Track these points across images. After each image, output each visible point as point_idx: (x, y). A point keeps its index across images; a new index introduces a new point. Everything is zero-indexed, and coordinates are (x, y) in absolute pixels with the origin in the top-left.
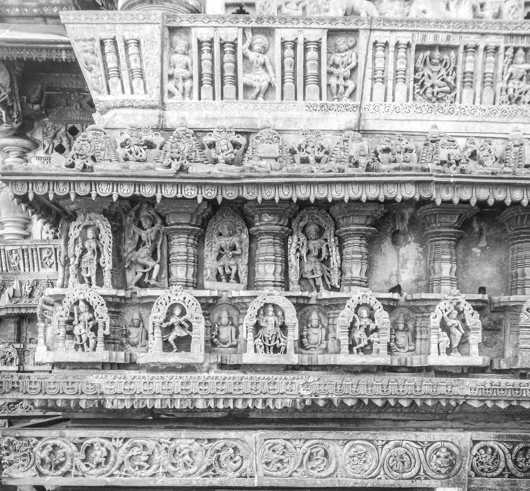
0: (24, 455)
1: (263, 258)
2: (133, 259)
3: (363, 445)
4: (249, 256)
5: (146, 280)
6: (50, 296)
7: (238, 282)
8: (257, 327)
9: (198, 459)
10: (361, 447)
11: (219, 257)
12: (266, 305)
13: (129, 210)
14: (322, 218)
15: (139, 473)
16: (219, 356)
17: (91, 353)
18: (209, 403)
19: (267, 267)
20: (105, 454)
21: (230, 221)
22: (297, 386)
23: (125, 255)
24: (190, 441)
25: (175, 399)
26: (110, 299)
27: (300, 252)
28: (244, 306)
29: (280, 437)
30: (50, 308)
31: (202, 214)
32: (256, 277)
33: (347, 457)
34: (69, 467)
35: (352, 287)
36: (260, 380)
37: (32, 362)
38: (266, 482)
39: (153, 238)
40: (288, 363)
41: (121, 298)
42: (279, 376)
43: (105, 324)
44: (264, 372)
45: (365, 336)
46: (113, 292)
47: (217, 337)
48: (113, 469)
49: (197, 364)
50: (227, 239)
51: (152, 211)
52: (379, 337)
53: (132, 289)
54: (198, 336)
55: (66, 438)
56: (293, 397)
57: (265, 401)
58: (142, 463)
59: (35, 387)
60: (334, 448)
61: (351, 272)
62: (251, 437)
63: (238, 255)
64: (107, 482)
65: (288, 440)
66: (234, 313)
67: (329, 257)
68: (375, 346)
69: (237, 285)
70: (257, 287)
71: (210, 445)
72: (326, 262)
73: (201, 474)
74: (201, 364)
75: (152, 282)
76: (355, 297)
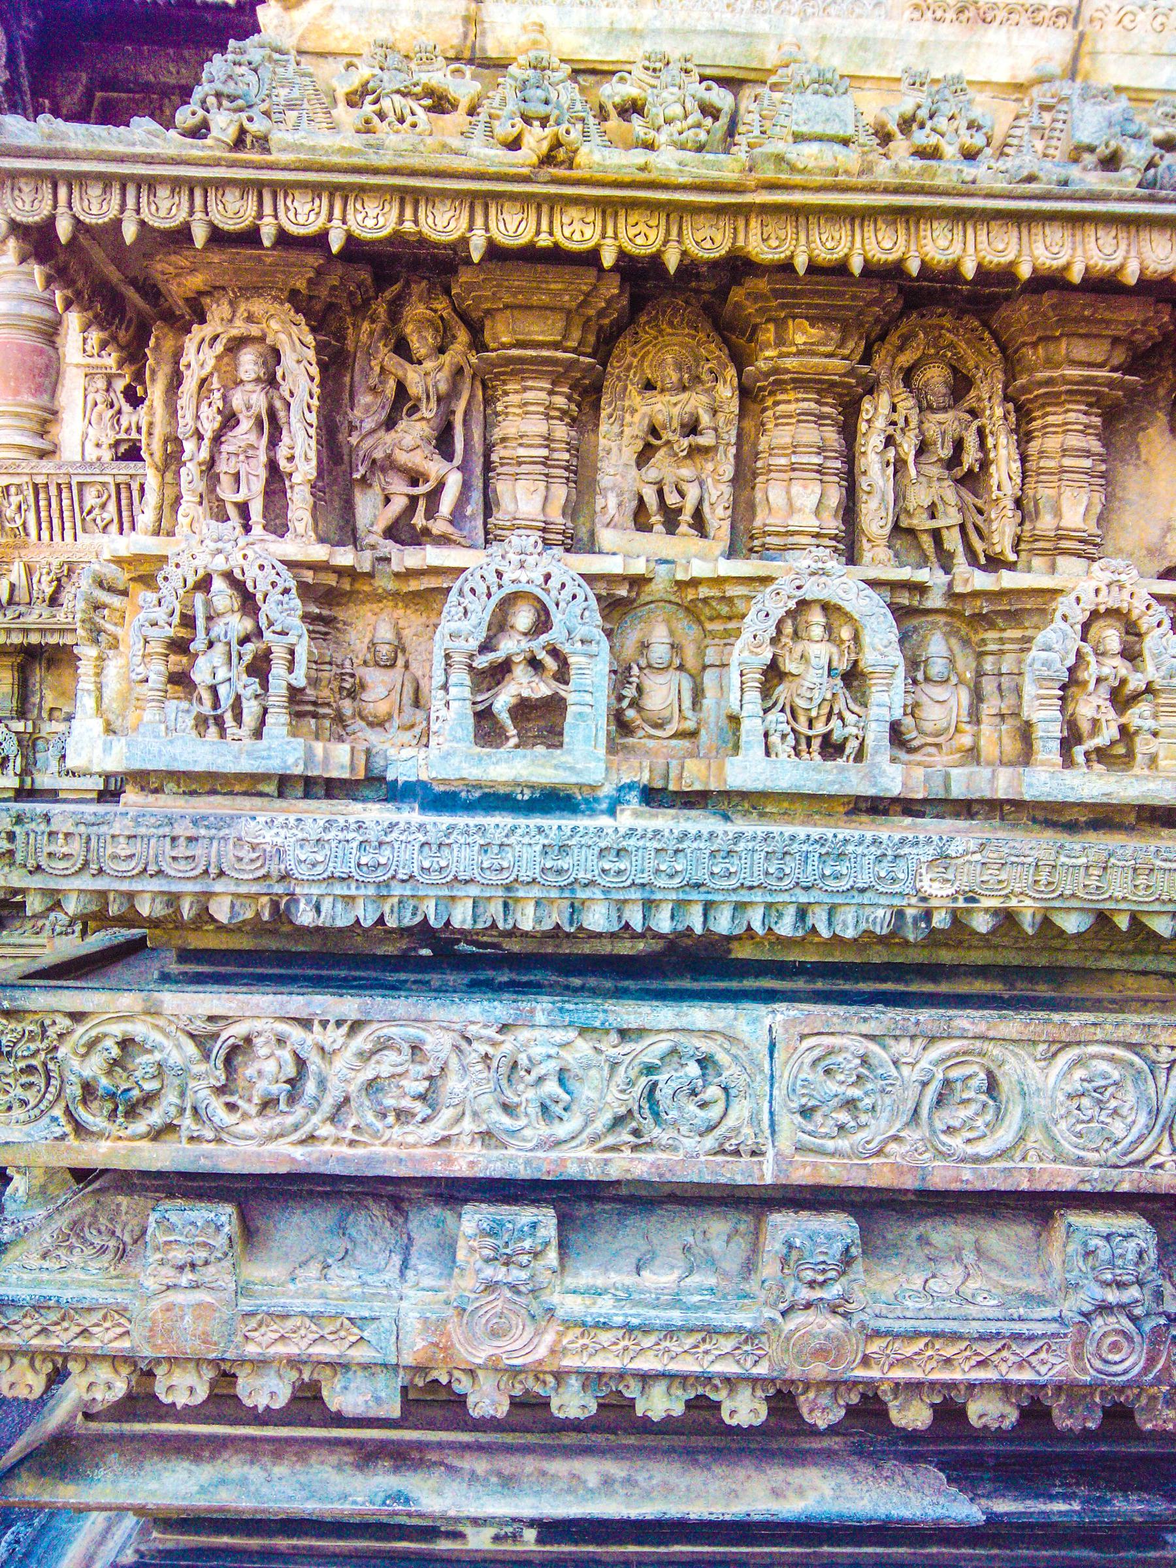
0: (30, 1070)
1: (783, 461)
2: (378, 455)
3: (1111, 1059)
4: (737, 457)
5: (419, 520)
6: (119, 561)
7: (704, 535)
8: (774, 673)
9: (587, 1092)
10: (1103, 1066)
11: (645, 456)
12: (803, 604)
13: (366, 303)
14: (968, 342)
15: (397, 1133)
16: (646, 763)
17: (247, 742)
18: (626, 916)
19: (796, 488)
20: (291, 1071)
21: (682, 345)
22: (913, 866)
23: (354, 440)
24: (560, 1036)
25: (517, 900)
26: (308, 576)
27: (895, 446)
28: (724, 610)
29: (848, 1030)
30: (115, 601)
31: (601, 313)
32: (758, 522)
33: (1061, 1097)
34: (173, 1111)
35: (1061, 561)
36: (795, 846)
37: (54, 766)
38: (801, 1172)
39: (443, 387)
40: (872, 792)
41: (340, 572)
42: (857, 834)
43: (292, 653)
44: (786, 816)
45: (1112, 714)
46: (319, 553)
47: (634, 704)
48: (315, 1119)
49: (580, 786)
50: (674, 399)
51: (441, 305)
52: (1155, 717)
53: (373, 547)
54: (588, 698)
55: (161, 1018)
56: (897, 901)
57: (802, 913)
58: (406, 1103)
59: (65, 850)
60: (1016, 1067)
61: (1057, 513)
62: (753, 1023)
63: (704, 451)
64: (294, 1160)
65: (871, 1038)
66: (688, 632)
67: (985, 464)
68: (1143, 746)
69: (702, 543)
70: (763, 552)
71: (626, 1048)
72: (972, 480)
73: (595, 1139)
74: (593, 788)
75: (439, 527)
76: (1086, 588)
